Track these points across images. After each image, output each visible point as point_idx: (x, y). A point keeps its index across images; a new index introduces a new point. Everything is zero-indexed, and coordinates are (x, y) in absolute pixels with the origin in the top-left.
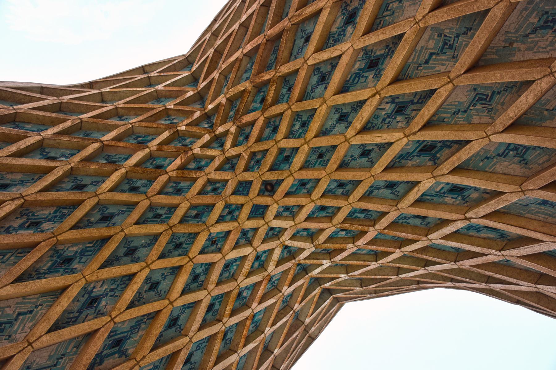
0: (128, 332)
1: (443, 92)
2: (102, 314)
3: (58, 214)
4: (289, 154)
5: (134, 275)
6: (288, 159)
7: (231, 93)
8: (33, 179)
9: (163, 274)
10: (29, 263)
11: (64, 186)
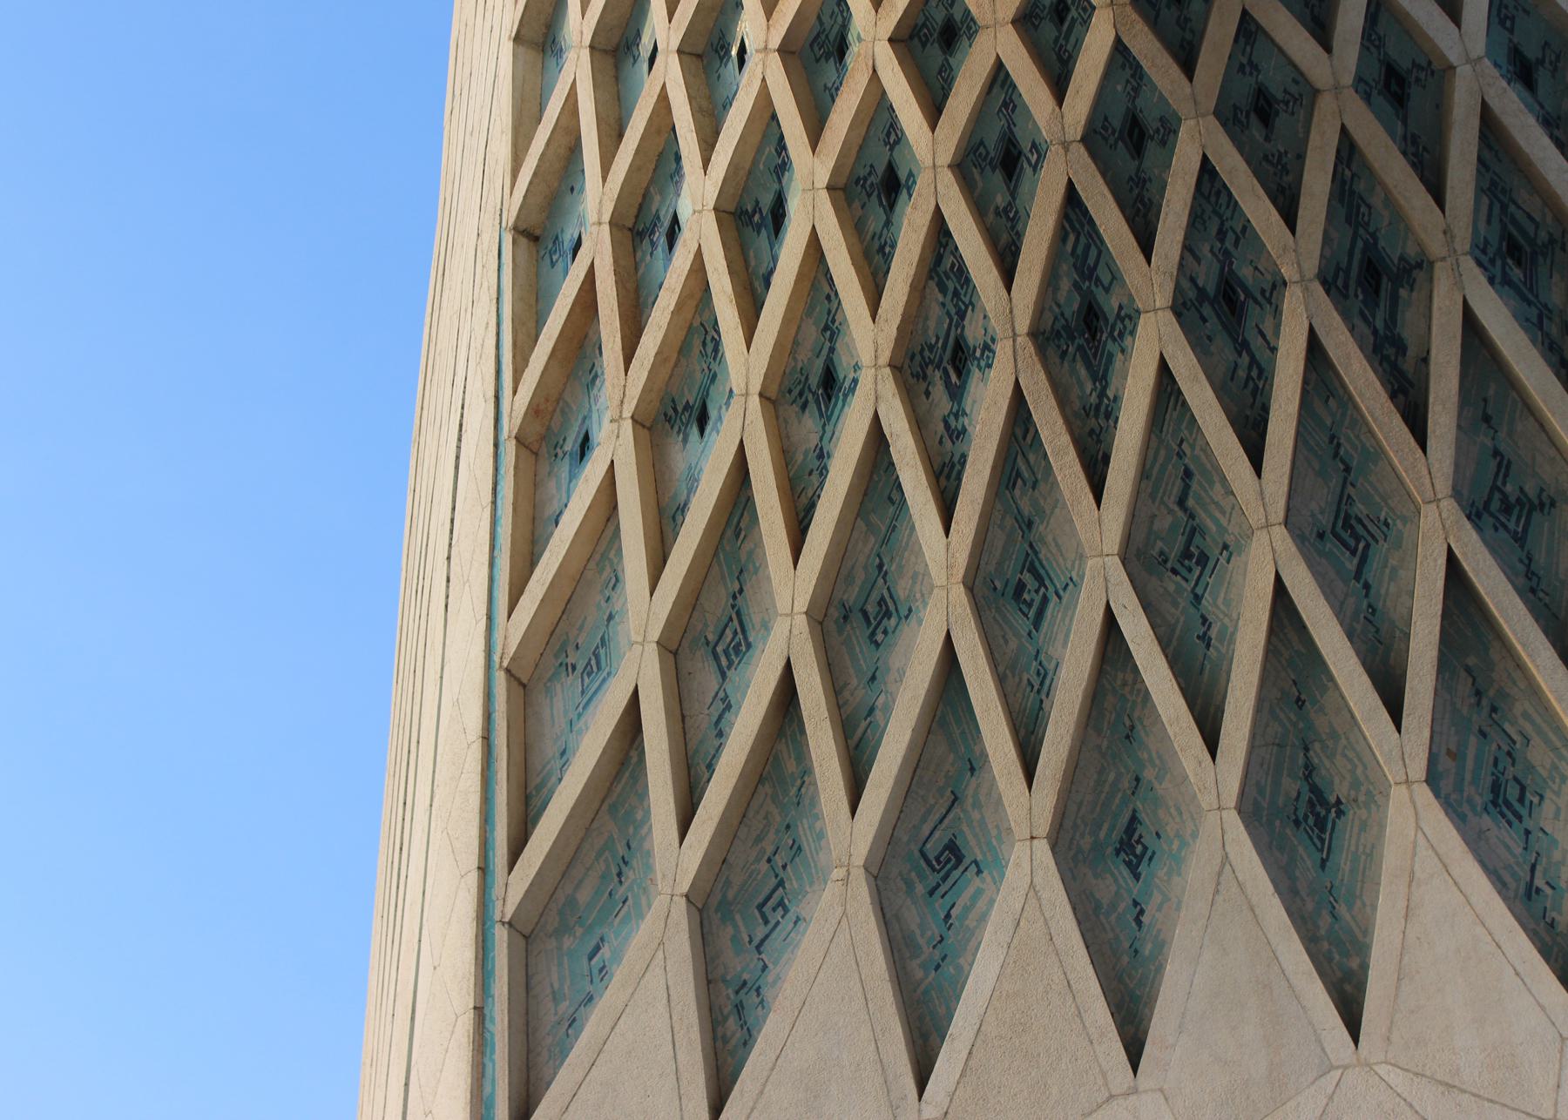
2: (1274, 286)
3: (951, 285)
8: (828, 298)
9: (1242, 68)
10: (1065, 439)
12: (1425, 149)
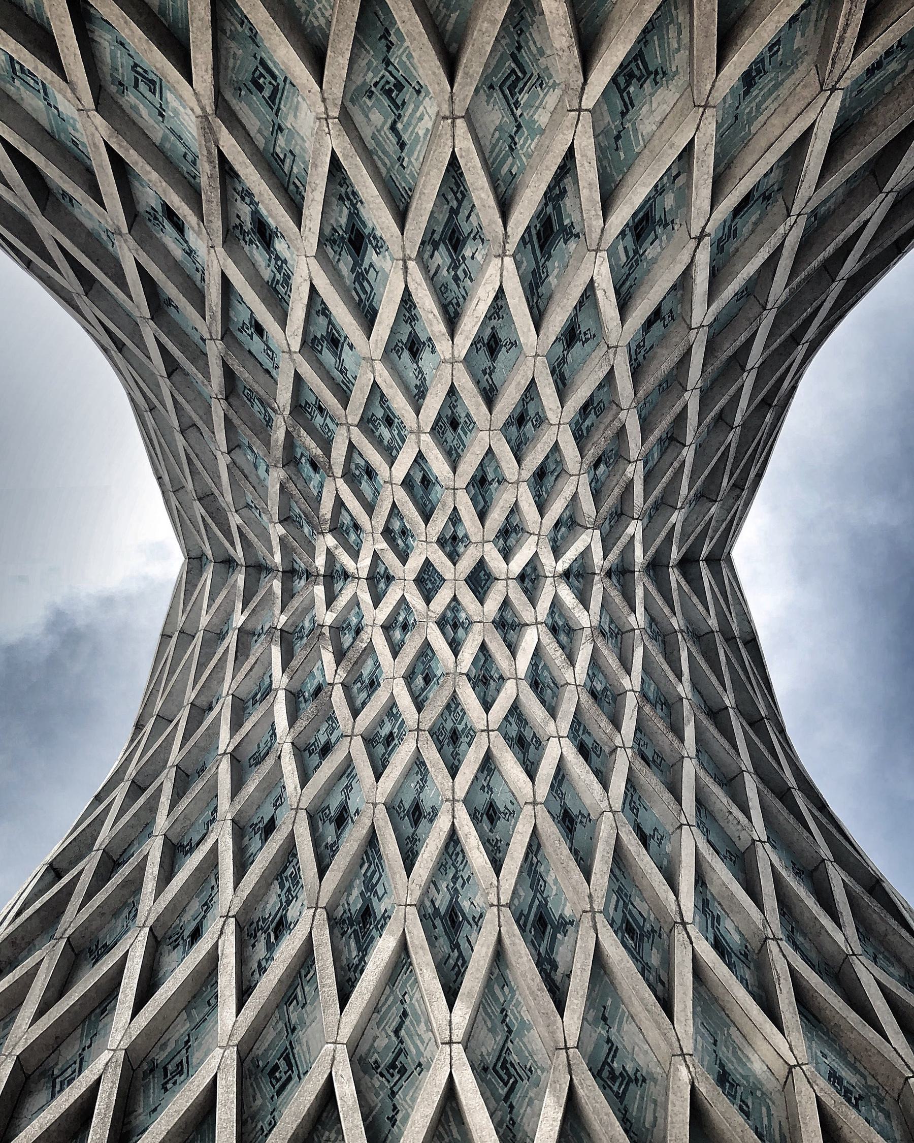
0: (534, 897)
1: (465, 146)
3: (287, 885)
4: (421, 474)
5: (453, 831)
6: (427, 482)
7: (274, 509)
9: (483, 788)
11: (252, 850)
12: (581, 858)
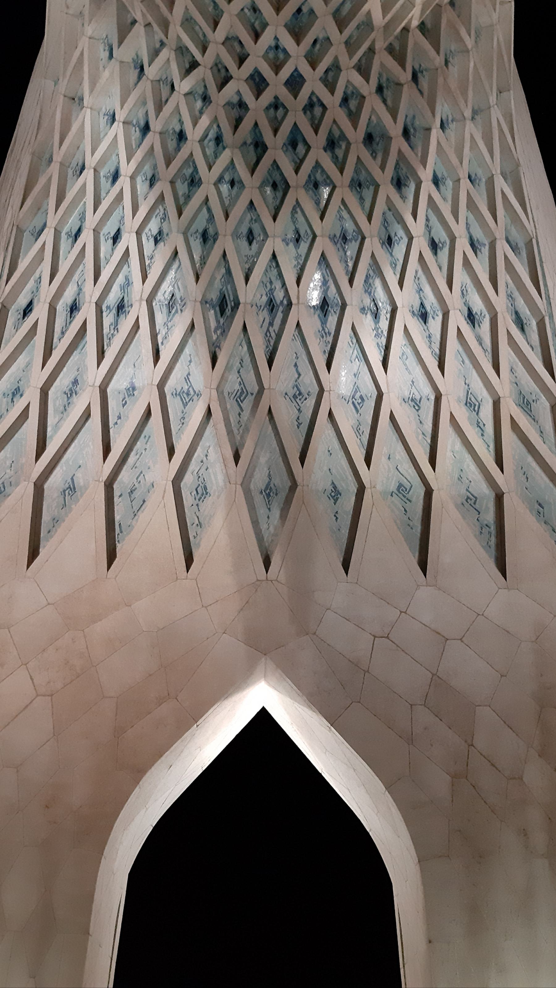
4: (297, 151)
